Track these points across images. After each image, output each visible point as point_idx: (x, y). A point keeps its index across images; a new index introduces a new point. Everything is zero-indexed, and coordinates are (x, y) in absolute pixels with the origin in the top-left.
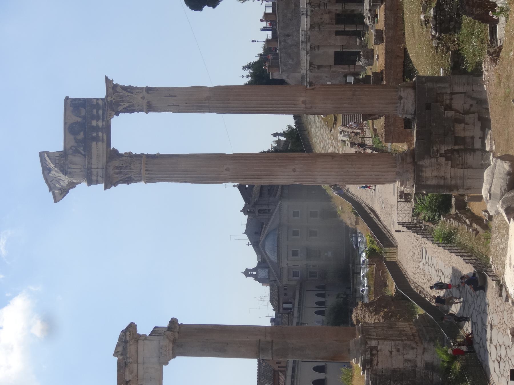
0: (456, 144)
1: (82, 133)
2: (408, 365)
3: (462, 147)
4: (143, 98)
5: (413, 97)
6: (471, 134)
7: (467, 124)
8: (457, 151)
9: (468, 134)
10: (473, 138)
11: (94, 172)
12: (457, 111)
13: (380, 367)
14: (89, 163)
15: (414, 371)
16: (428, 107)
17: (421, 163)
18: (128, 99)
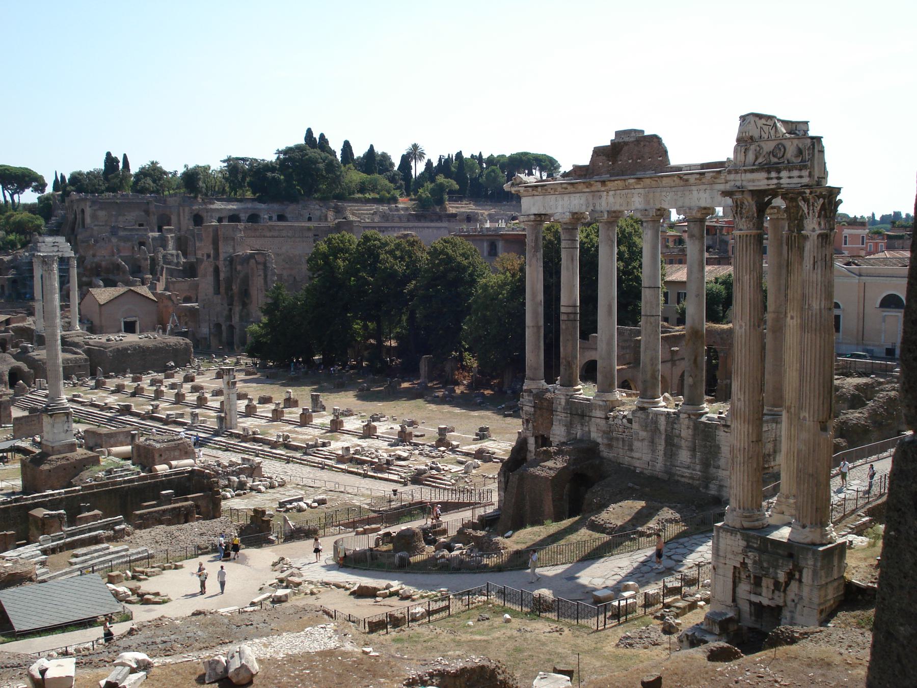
0: (755, 577)
1: (776, 160)
2: (722, 462)
3: (752, 581)
4: (814, 230)
5: (802, 541)
6: (763, 594)
8: (749, 576)
9: (764, 590)
10: (760, 595)
12: (787, 584)
13: (722, 433)
14: (745, 171)
16: (791, 556)
17: (739, 536)
18: (811, 212)
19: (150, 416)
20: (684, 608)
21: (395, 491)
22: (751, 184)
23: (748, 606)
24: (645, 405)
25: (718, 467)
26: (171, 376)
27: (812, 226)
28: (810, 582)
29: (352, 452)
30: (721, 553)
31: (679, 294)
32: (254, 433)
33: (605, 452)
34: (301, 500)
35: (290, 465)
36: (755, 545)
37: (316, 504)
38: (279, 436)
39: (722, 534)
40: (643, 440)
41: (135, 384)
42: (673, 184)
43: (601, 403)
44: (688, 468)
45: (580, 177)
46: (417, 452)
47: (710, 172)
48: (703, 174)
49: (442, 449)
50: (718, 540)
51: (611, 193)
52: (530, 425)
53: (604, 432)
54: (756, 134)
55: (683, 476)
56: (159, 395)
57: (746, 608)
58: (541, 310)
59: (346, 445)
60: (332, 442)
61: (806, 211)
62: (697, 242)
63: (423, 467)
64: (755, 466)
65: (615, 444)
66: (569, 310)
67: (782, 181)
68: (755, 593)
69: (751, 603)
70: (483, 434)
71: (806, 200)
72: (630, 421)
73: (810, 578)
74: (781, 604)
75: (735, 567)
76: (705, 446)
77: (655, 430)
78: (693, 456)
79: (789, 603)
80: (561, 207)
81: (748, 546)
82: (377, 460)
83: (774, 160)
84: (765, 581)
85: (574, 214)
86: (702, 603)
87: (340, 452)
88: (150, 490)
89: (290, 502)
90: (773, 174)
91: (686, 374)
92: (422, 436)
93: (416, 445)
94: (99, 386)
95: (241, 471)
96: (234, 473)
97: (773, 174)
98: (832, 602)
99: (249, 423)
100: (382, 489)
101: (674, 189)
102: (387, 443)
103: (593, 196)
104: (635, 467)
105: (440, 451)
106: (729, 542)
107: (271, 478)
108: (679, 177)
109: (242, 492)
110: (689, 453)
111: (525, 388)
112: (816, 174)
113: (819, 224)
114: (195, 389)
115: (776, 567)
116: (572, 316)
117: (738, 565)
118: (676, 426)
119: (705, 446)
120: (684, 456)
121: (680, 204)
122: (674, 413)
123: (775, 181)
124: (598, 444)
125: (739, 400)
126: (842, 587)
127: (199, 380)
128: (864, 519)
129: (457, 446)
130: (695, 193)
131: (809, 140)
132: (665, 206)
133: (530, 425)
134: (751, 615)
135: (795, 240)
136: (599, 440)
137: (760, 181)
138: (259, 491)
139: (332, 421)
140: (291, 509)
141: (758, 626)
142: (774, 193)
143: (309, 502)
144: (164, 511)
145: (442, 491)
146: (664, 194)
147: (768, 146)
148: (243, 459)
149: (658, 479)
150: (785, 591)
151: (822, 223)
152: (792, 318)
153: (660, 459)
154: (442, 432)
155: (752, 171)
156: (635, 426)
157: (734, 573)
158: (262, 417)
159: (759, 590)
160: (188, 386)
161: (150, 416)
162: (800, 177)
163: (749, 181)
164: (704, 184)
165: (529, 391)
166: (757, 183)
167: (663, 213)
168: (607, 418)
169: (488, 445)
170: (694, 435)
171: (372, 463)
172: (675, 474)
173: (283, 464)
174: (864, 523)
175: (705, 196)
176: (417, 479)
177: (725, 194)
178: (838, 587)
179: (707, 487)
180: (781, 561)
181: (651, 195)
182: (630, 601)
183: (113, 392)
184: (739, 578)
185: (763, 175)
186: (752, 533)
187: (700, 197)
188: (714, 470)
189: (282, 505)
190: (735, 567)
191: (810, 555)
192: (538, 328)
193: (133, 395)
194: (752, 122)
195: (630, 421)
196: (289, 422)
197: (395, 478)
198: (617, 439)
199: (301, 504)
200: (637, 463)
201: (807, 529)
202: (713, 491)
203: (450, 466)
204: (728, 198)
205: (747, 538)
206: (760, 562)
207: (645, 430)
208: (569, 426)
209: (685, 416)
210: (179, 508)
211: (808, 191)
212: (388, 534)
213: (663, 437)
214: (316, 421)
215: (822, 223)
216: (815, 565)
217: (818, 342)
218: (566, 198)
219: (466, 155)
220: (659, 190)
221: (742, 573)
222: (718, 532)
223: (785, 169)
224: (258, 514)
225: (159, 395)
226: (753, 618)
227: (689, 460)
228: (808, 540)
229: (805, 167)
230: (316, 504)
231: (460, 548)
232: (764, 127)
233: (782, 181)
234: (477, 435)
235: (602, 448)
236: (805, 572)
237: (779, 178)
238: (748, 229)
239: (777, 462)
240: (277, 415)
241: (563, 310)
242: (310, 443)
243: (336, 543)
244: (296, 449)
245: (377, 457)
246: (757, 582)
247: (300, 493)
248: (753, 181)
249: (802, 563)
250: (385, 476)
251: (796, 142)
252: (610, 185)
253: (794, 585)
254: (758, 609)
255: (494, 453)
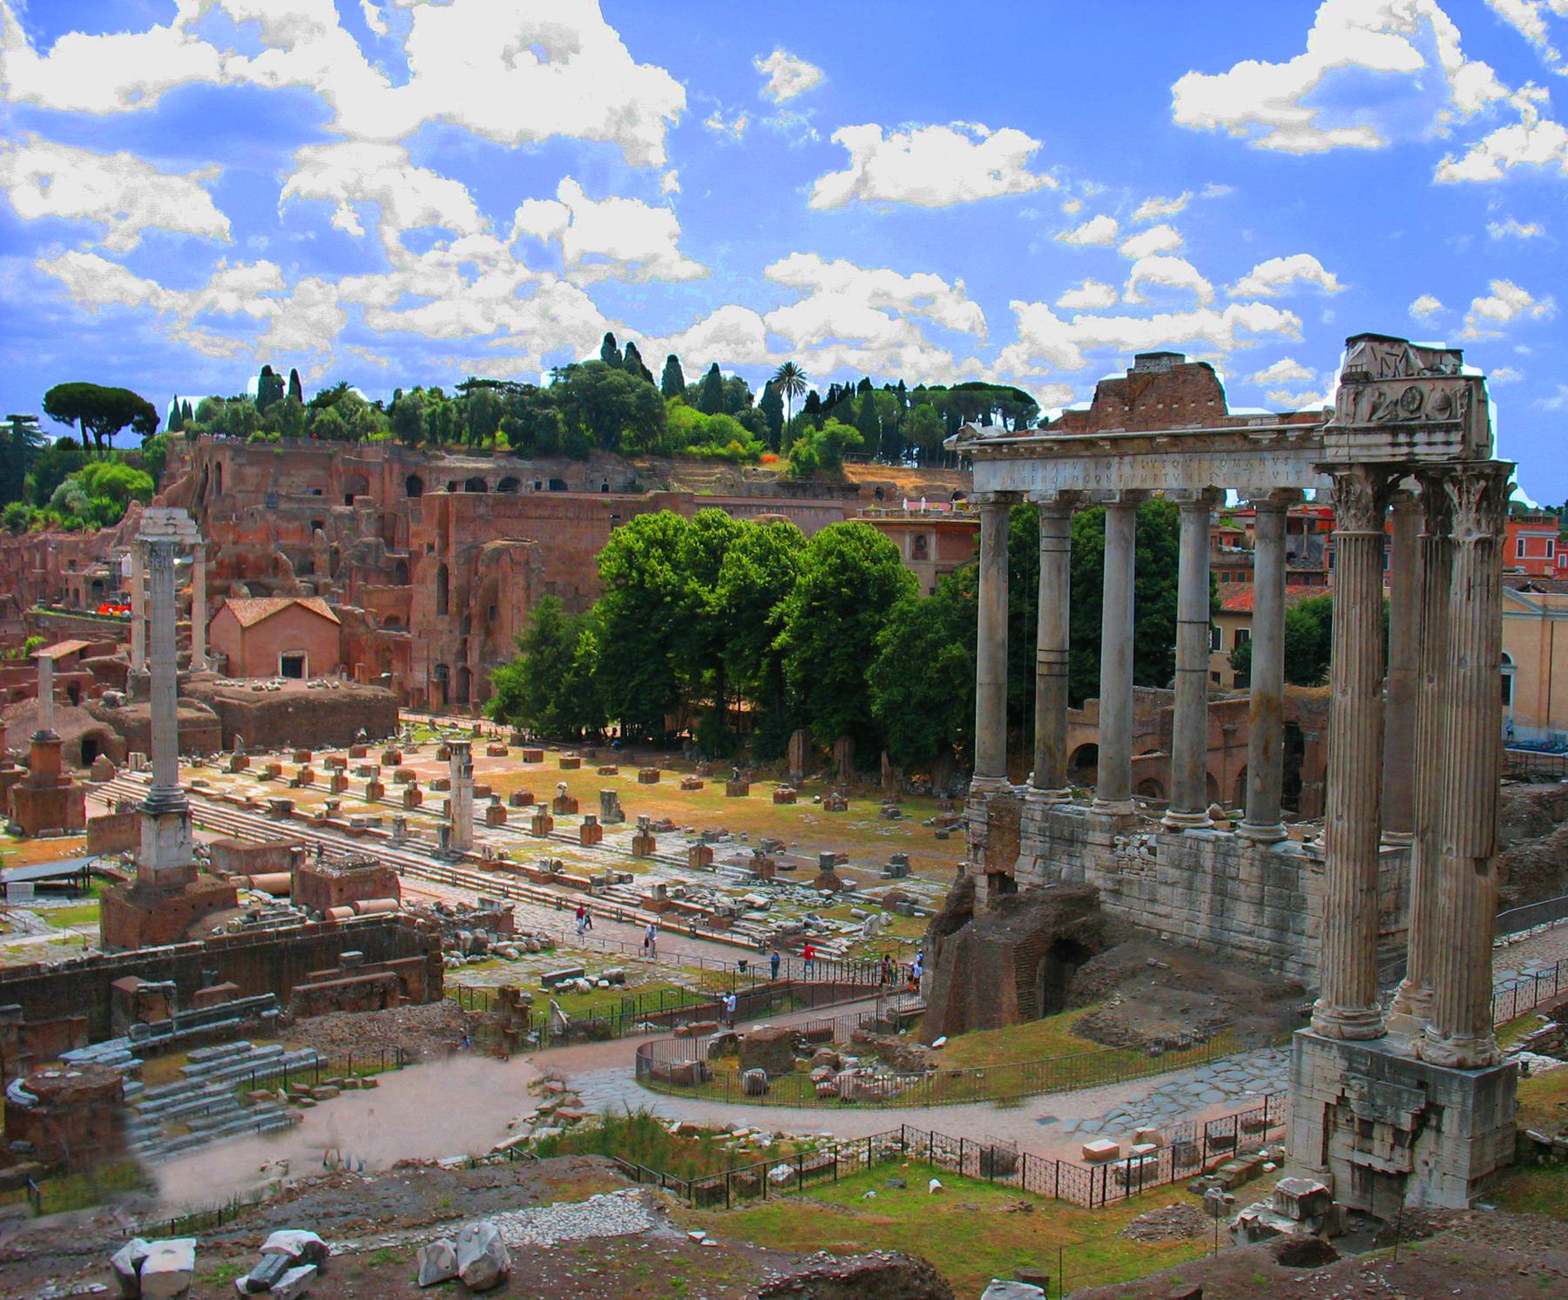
2: (1309, 923)
6: (1376, 1152)
7: (1392, 1148)
8: (1352, 1120)
10: (1370, 1152)
11: (1343, 440)
12: (1416, 1134)
13: (1308, 874)
14: (1356, 431)
15: (1301, 933)
16: (1422, 1085)
17: (1335, 1052)
19: (322, 823)
20: (1239, 1174)
21: (743, 964)
22: (1365, 452)
23: (1349, 1170)
24: (1180, 824)
25: (1301, 933)
26: (361, 754)
27: (1466, 528)
28: (1455, 1132)
29: (669, 894)
30: (1305, 1081)
31: (1238, 633)
32: (501, 857)
33: (1109, 906)
34: (580, 974)
35: (562, 914)
36: (1363, 1068)
37: (606, 983)
38: (544, 863)
39: (1306, 1047)
40: (1173, 884)
41: (300, 767)
42: (1232, 447)
43: (1104, 819)
44: (1250, 934)
45: (1075, 429)
46: (782, 897)
47: (1295, 434)
48: (1283, 431)
49: (826, 892)
50: (1299, 1058)
51: (1127, 459)
52: (980, 854)
53: (1109, 870)
54: (1374, 372)
55: (1240, 948)
56: (340, 784)
57: (1344, 1175)
58: (1003, 655)
59: (659, 881)
60: (636, 877)
61: (1456, 501)
62: (1272, 547)
63: (791, 924)
64: (1364, 932)
65: (1125, 890)
66: (1051, 657)
67: (1417, 450)
68: (1361, 1150)
69: (1355, 1166)
70: (900, 869)
71: (1456, 482)
72: (1152, 851)
73: (1455, 1125)
74: (1406, 1169)
75: (1327, 1105)
76: (1280, 897)
77: (1195, 868)
78: (1260, 912)
79: (1419, 1167)
80: (1042, 483)
81: (1350, 1069)
82: (712, 909)
83: (1402, 414)
84: (1377, 1132)
85: (1062, 493)
86: (1270, 1165)
87: (649, 894)
88: (321, 946)
89: (562, 977)
90: (1402, 438)
91: (1250, 772)
92: (790, 869)
93: (780, 884)
94: (238, 766)
95: (479, 922)
96: (464, 924)
97: (1402, 438)
98: (1492, 1167)
99: (494, 839)
100: (721, 960)
101: (1234, 456)
102: (729, 881)
103: (1097, 464)
104: (1160, 931)
105: (821, 895)
106: (1318, 1061)
107: (529, 935)
108: (1244, 435)
109: (478, 958)
110: (1252, 908)
111: (972, 790)
112: (1474, 439)
113: (1478, 522)
114: (404, 777)
115: (1398, 1107)
116: (1056, 669)
117: (1333, 1102)
118: (1230, 860)
119: (1280, 897)
120: (1243, 914)
121: (1243, 481)
122: (1228, 839)
123: (1405, 450)
124: (1097, 890)
125: (1339, 818)
126: (1511, 1140)
127: (408, 761)
128: (1547, 1027)
129: (853, 888)
130: (1269, 463)
131: (1462, 383)
132: (1219, 484)
133: (980, 854)
134: (1353, 1187)
135: (1440, 551)
136: (1099, 883)
137: (1381, 449)
138: (508, 957)
139: (635, 840)
140: (565, 989)
141: (1366, 1207)
142: (1404, 469)
143: (595, 979)
144: (345, 987)
145: (824, 966)
146: (1217, 463)
147: (1395, 391)
148: (482, 901)
149: (1197, 949)
150: (1412, 1146)
151: (1483, 522)
152: (1431, 680)
153: (1204, 917)
154: (827, 863)
155: (1367, 431)
156: (1160, 859)
157: (1326, 1115)
158: (514, 830)
159: (1367, 1144)
160: (390, 771)
161: (322, 823)
162: (1448, 443)
163: (1362, 446)
164: (1284, 449)
165: (979, 794)
166: (1374, 452)
167: (1213, 496)
168: (1113, 846)
169: (908, 886)
170: (1262, 880)
171: (705, 914)
172: (1226, 944)
173: (551, 910)
174: (1548, 1033)
175: (1287, 468)
176: (785, 941)
177: (1322, 468)
178: (1503, 1142)
179: (1281, 968)
180: (1405, 1096)
181: (1195, 464)
182: (1147, 1160)
183: (262, 779)
184: (1335, 1124)
185: (1386, 438)
186: (1357, 1045)
187: (1278, 473)
188: (1295, 938)
189: (548, 982)
190: (1327, 1105)
191: (1456, 1085)
192: (998, 687)
193: (295, 784)
194: (1368, 350)
195: (1152, 851)
196: (564, 840)
197: (744, 940)
198: (1130, 882)
199: (581, 981)
200: (1162, 924)
201: (1450, 1041)
202: (1291, 973)
203: (838, 923)
204: (1325, 475)
205: (1349, 1055)
206: (1372, 1097)
207: (1178, 867)
208: (1047, 857)
209: (1247, 843)
210: (376, 980)
211: (1459, 467)
212: (732, 1038)
213: (1209, 879)
214: (609, 839)
215: (1483, 522)
216: (1463, 1104)
217: (1474, 723)
218: (1050, 465)
219: (878, 384)
220: (1208, 456)
221: (1340, 1116)
222: (1300, 1044)
223: (1423, 428)
224: (509, 996)
225: (340, 784)
226: (1357, 1193)
227: (1252, 920)
228: (1453, 1059)
229: (1456, 427)
230: (606, 983)
231: (854, 1066)
232: (1388, 358)
233: (1417, 450)
234: (887, 869)
235: (1102, 896)
236: (1446, 1113)
237: (1412, 445)
238: (1359, 527)
239: (1401, 926)
240: (542, 826)
241: (1041, 656)
242: (597, 876)
243: (640, 1050)
244: (575, 885)
245: (712, 904)
246: (1365, 1130)
247: (579, 963)
248: (1369, 446)
249: (1442, 1100)
250: (727, 936)
251: (1440, 385)
252: (1127, 447)
253: (1428, 1136)
254: (1367, 1176)
255: (915, 902)
